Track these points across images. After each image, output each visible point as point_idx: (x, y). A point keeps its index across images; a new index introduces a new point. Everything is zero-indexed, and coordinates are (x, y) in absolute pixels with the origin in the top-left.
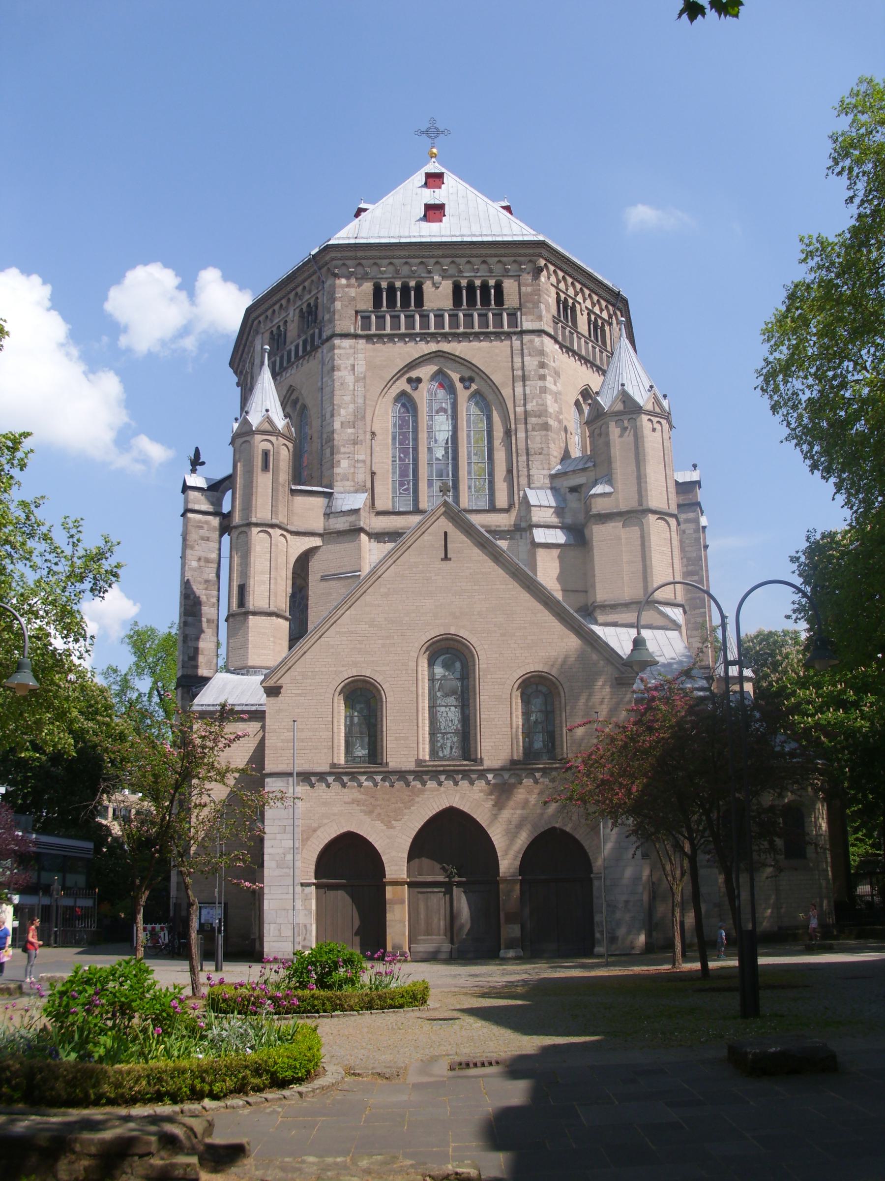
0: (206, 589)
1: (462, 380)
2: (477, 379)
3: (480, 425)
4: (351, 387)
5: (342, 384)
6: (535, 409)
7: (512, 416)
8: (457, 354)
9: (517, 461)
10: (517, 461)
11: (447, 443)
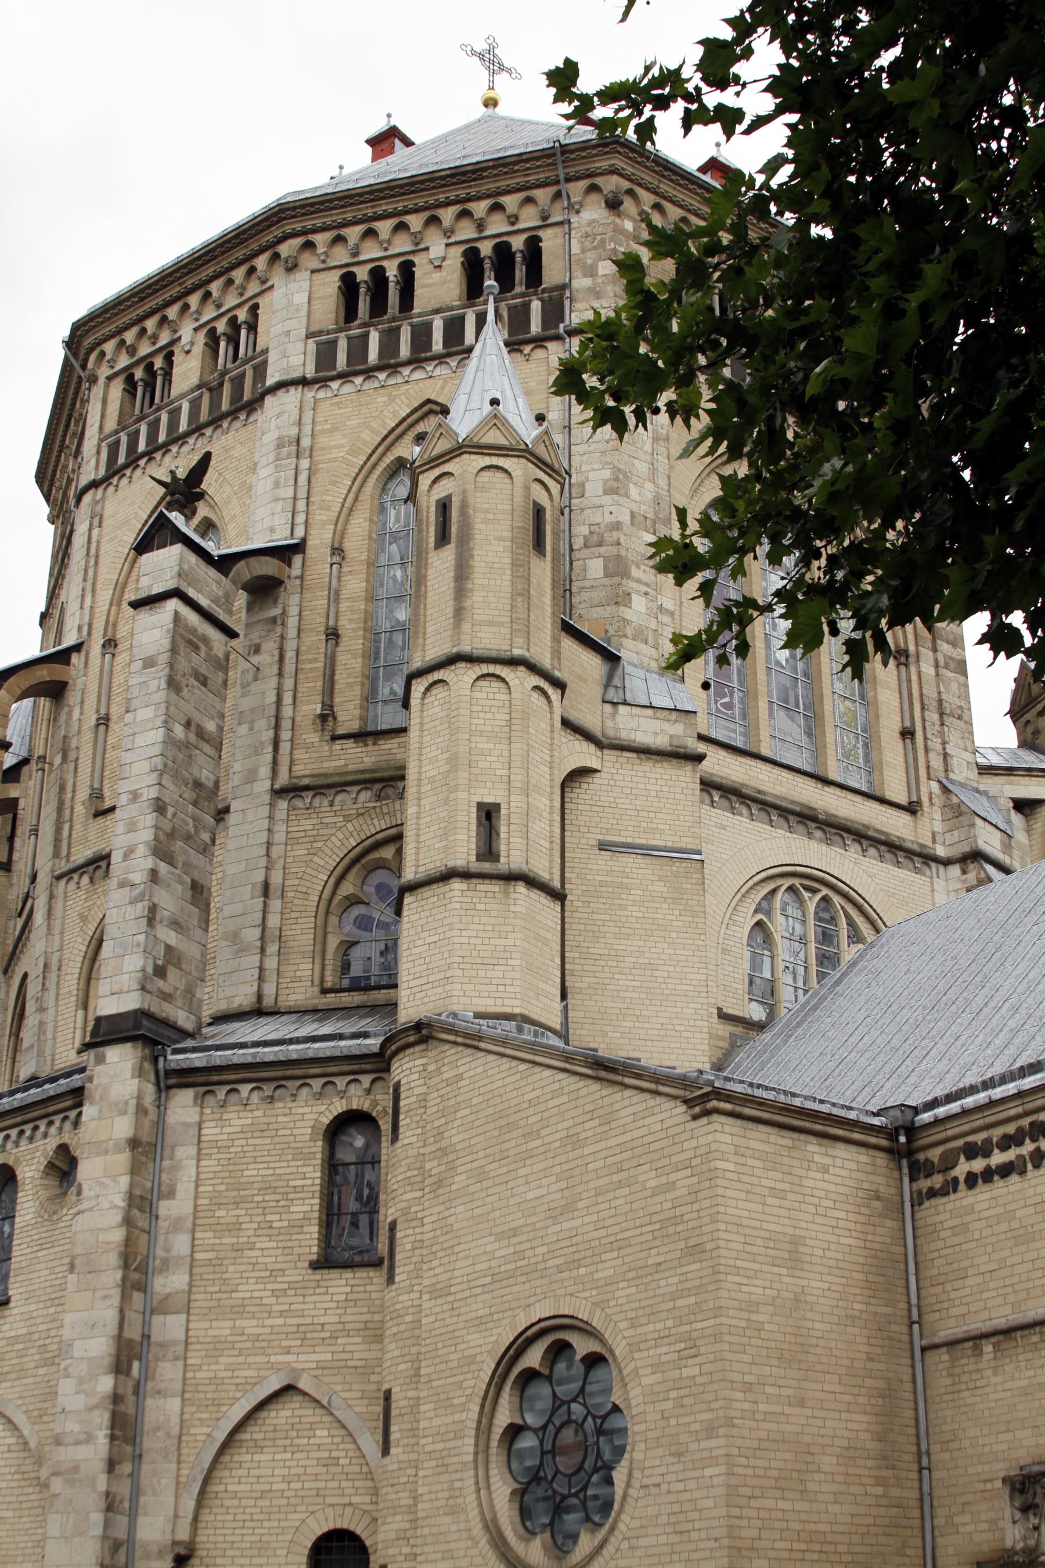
0: (195, 804)
4: (648, 448)
9: (924, 720)
10: (924, 720)
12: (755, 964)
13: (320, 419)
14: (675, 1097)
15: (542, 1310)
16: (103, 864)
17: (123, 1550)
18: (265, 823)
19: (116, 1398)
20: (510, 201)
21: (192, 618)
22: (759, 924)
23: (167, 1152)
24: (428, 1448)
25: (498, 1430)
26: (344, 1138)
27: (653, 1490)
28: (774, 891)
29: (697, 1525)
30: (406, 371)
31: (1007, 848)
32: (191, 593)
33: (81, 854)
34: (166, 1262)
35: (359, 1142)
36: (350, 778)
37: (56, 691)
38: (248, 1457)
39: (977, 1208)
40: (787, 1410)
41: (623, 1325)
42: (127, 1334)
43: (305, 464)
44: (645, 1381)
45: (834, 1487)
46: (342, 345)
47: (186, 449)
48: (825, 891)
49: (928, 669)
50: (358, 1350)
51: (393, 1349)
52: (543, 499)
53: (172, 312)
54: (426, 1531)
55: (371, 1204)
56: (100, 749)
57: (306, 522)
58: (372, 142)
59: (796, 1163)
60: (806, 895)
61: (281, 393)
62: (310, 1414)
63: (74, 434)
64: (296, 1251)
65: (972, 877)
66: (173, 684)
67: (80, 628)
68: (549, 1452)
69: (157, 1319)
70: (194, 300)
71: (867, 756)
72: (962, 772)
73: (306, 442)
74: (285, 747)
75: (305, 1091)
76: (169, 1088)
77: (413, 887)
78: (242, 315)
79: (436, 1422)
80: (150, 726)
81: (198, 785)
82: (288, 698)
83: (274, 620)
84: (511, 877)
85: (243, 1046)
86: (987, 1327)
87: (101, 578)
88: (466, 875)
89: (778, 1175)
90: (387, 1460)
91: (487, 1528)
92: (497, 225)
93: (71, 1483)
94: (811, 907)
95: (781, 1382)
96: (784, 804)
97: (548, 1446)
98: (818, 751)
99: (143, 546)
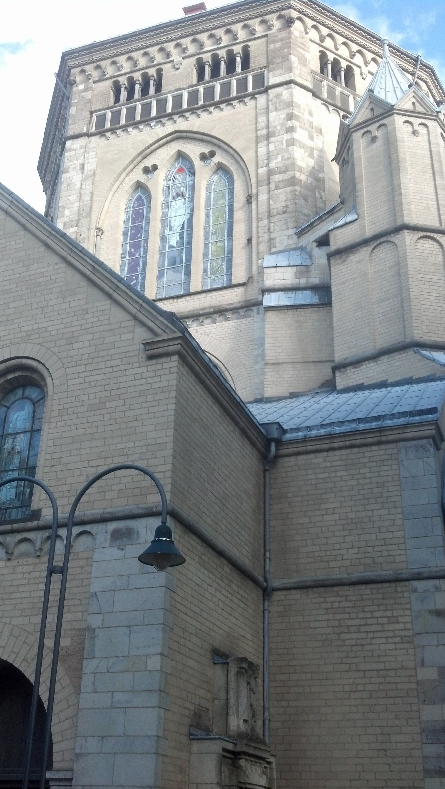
3: (221, 202)
4: (78, 186)
5: (69, 185)
6: (280, 165)
7: (253, 180)
8: (195, 129)
11: (183, 228)
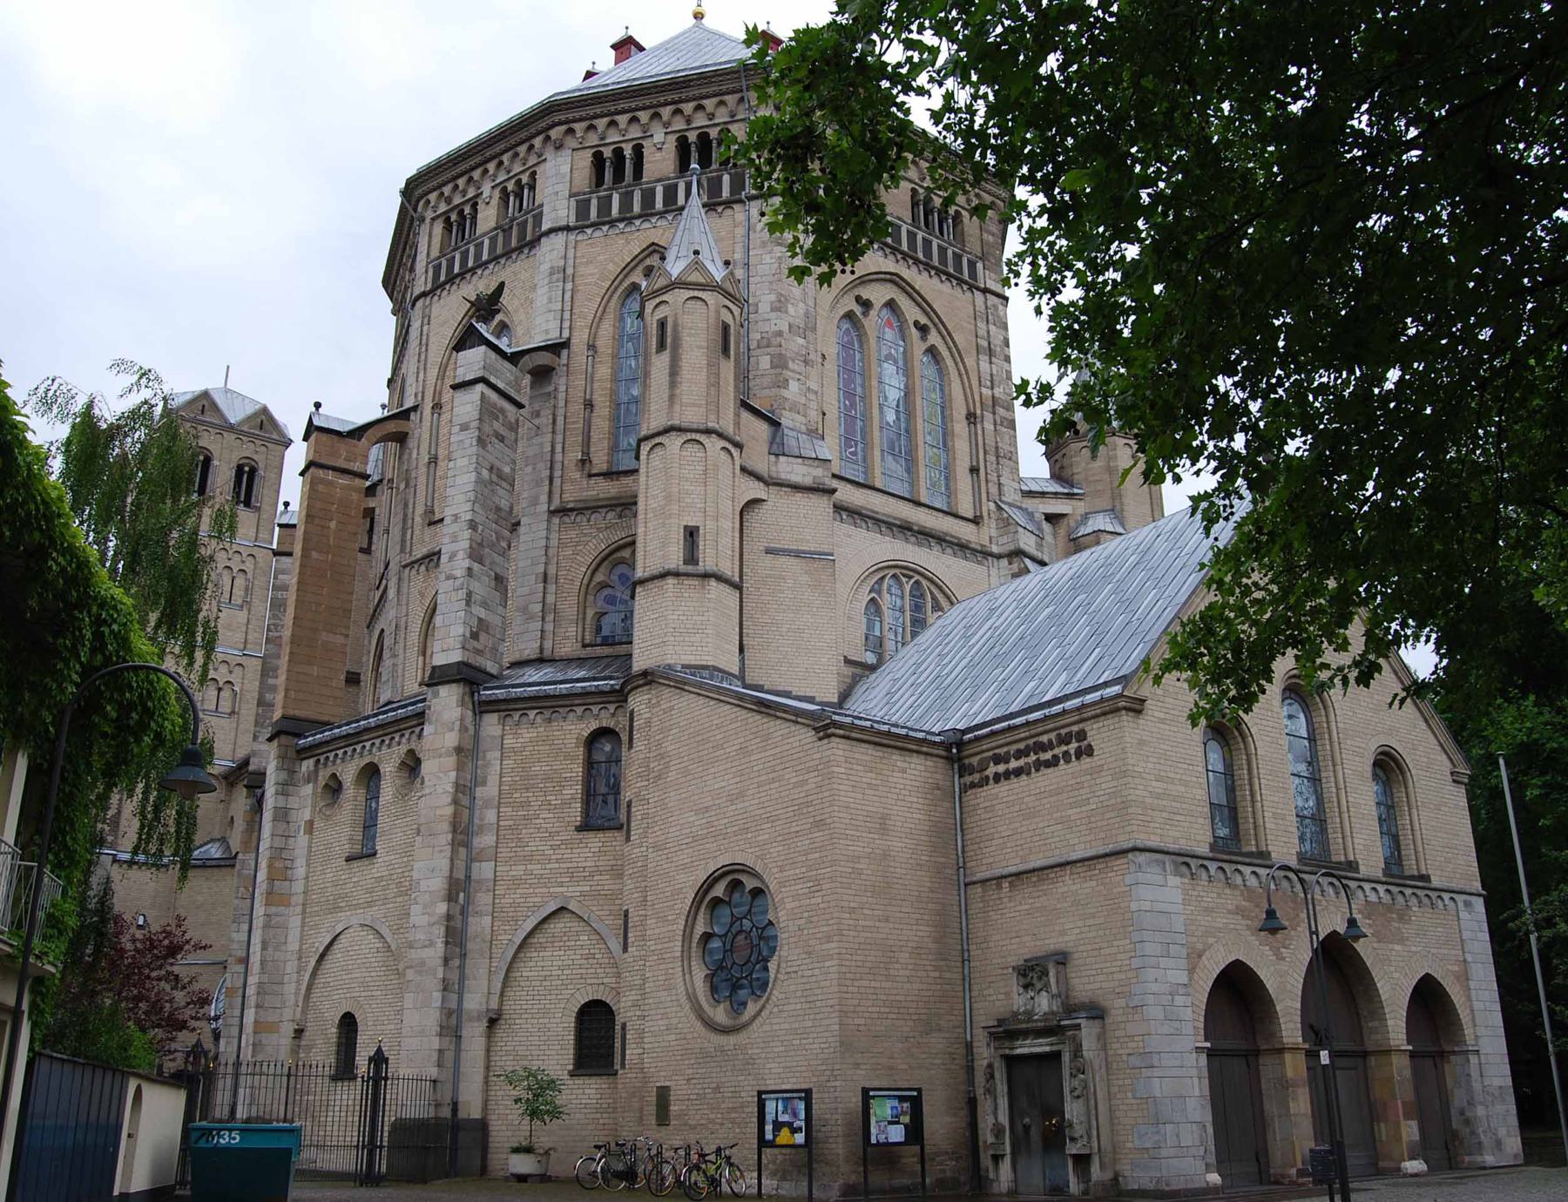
1: (916, 324)
2: (933, 332)
7: (977, 398)
11: (898, 406)
12: (870, 626)
13: (578, 255)
14: (808, 726)
15: (725, 860)
16: (435, 558)
17: (454, 1016)
18: (544, 533)
19: (449, 917)
20: (709, 104)
21: (493, 396)
22: (873, 600)
23: (481, 755)
24: (652, 948)
25: (696, 937)
26: (598, 745)
27: (793, 975)
28: (883, 578)
29: (820, 997)
30: (637, 222)
31: (1040, 546)
32: (493, 380)
33: (419, 552)
34: (481, 827)
35: (608, 748)
36: (600, 504)
37: (401, 438)
38: (535, 954)
39: (1000, 795)
40: (877, 924)
41: (775, 870)
42: (455, 875)
43: (569, 286)
44: (788, 906)
45: (907, 973)
46: (594, 202)
47: (487, 272)
48: (917, 577)
49: (989, 426)
50: (606, 882)
51: (629, 884)
52: (729, 319)
53: (476, 174)
54: (651, 1001)
55: (616, 789)
56: (432, 478)
57: (570, 328)
58: (615, 47)
59: (885, 767)
60: (904, 580)
61: (552, 236)
62: (575, 925)
63: (409, 256)
64: (567, 819)
65: (1015, 568)
66: (481, 442)
67: (416, 395)
68: (729, 950)
69: (475, 865)
70: (491, 166)
71: (948, 487)
72: (1011, 495)
73: (570, 271)
74: (557, 482)
75: (571, 714)
76: (481, 712)
77: (642, 582)
78: (525, 179)
79: (657, 931)
80: (465, 470)
81: (498, 509)
82: (559, 448)
83: (549, 394)
84: (706, 576)
85: (530, 685)
86: (1006, 871)
87: (430, 360)
88: (676, 574)
89: (873, 775)
90: (626, 955)
91: (689, 998)
92: (700, 120)
93: (420, 973)
94: (908, 588)
95: (874, 907)
96: (890, 520)
97: (728, 947)
98: (913, 483)
99: (459, 346)
